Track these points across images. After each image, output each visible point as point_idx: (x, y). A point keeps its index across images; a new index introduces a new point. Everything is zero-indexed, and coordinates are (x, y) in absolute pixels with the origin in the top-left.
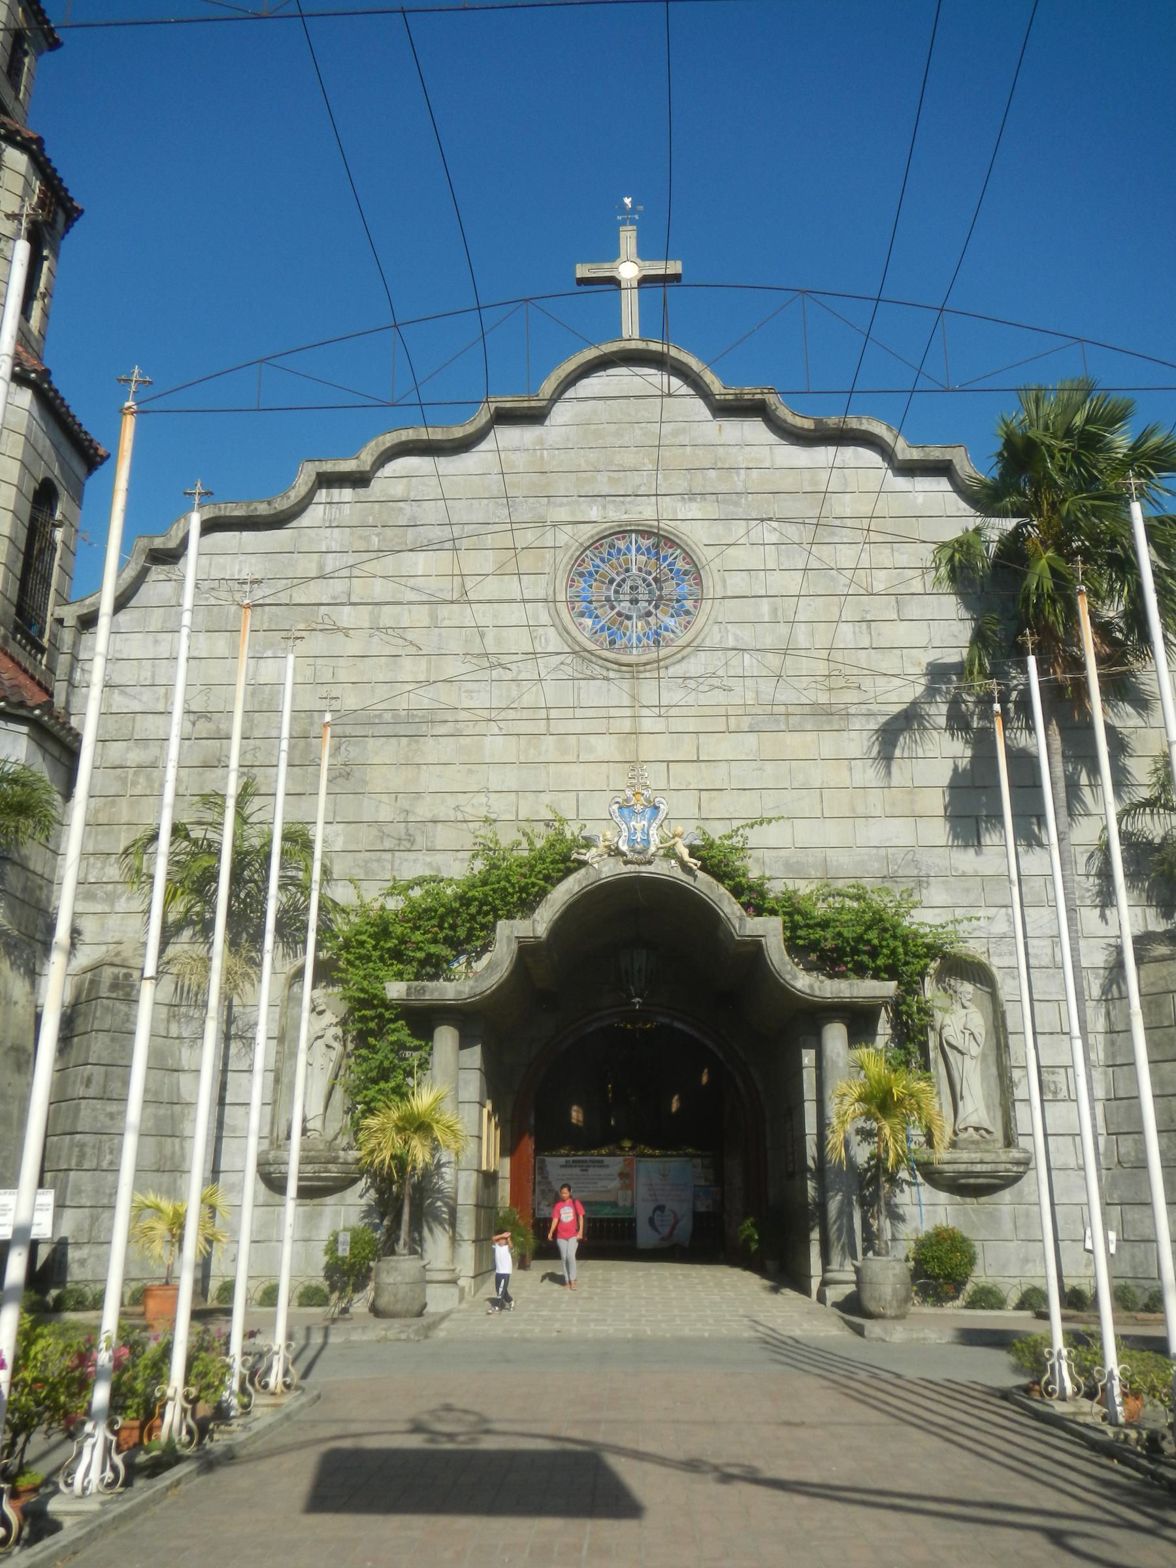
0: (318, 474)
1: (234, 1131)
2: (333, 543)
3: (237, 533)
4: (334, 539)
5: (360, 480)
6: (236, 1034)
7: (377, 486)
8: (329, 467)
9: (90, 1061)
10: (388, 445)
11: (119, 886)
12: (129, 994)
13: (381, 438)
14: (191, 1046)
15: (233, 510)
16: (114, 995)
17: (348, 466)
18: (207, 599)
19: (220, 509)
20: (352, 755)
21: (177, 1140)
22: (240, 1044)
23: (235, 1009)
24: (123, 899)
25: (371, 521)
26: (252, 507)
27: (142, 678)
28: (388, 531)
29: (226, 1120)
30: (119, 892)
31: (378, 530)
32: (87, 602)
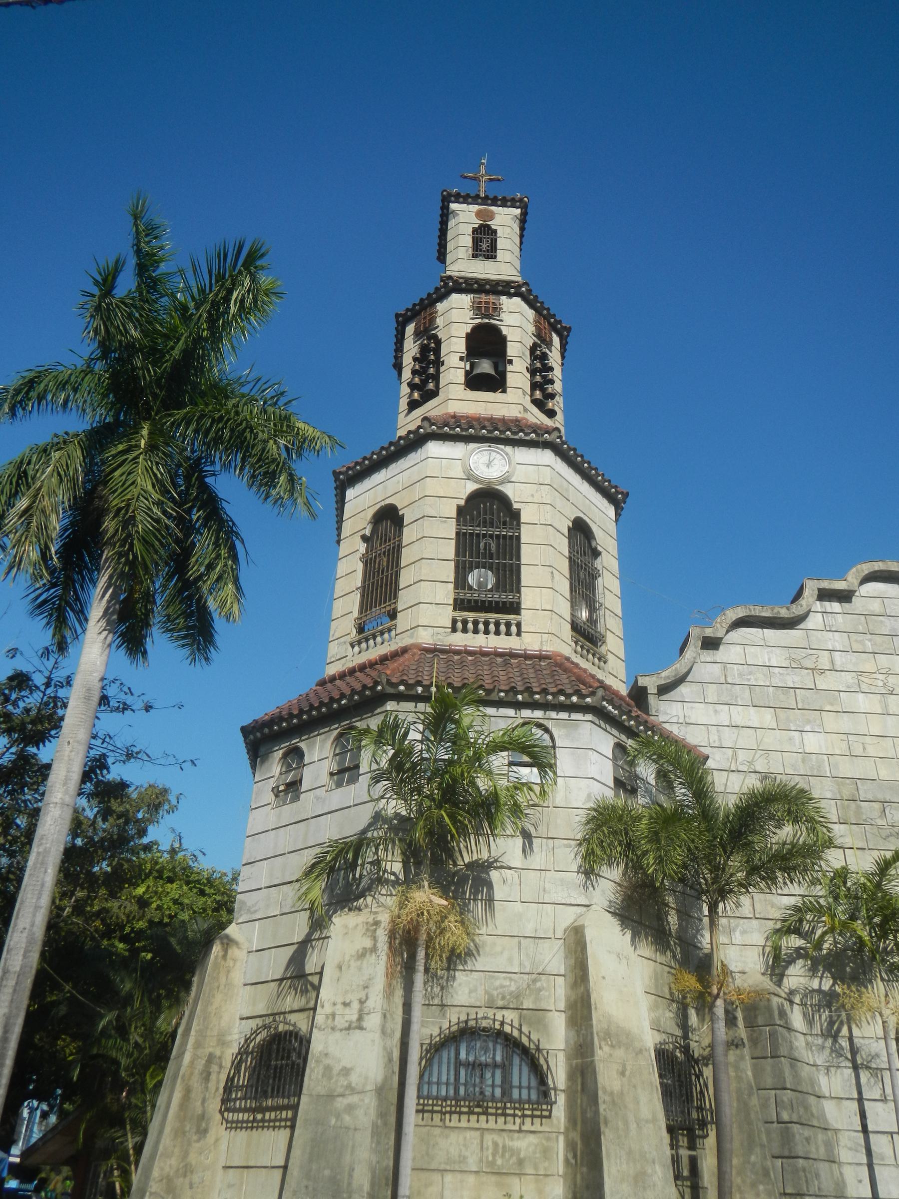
0: (819, 590)
1: (883, 1159)
2: (837, 644)
3: (760, 630)
4: (837, 641)
5: (844, 597)
6: (862, 1064)
7: (857, 603)
8: (825, 584)
9: (788, 1086)
10: (866, 572)
11: (732, 921)
12: (786, 1022)
13: (859, 566)
14: (827, 1074)
15: (760, 612)
16: (781, 1023)
17: (840, 585)
18: (749, 680)
19: (750, 610)
20: (895, 818)
21: (835, 1166)
22: (867, 1073)
23: (856, 1040)
24: (738, 933)
25: (861, 629)
26: (775, 611)
27: (711, 741)
28: (878, 639)
29: (873, 1148)
30: (733, 925)
31: (869, 636)
32: (663, 674)
